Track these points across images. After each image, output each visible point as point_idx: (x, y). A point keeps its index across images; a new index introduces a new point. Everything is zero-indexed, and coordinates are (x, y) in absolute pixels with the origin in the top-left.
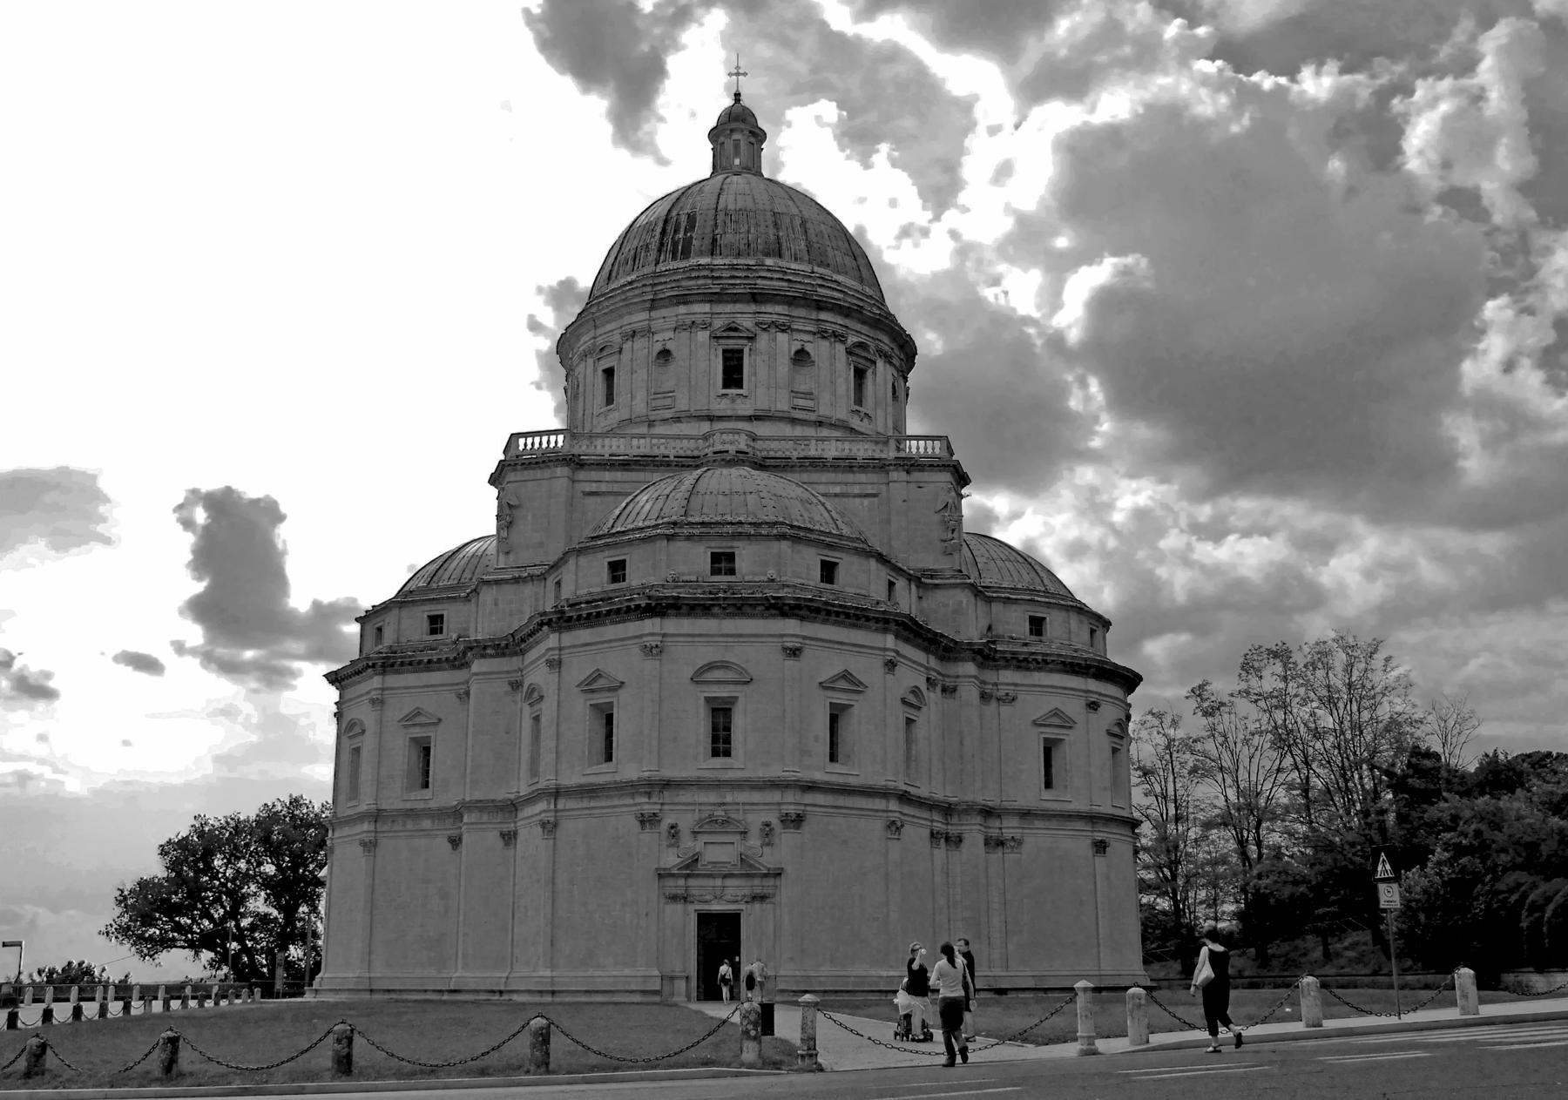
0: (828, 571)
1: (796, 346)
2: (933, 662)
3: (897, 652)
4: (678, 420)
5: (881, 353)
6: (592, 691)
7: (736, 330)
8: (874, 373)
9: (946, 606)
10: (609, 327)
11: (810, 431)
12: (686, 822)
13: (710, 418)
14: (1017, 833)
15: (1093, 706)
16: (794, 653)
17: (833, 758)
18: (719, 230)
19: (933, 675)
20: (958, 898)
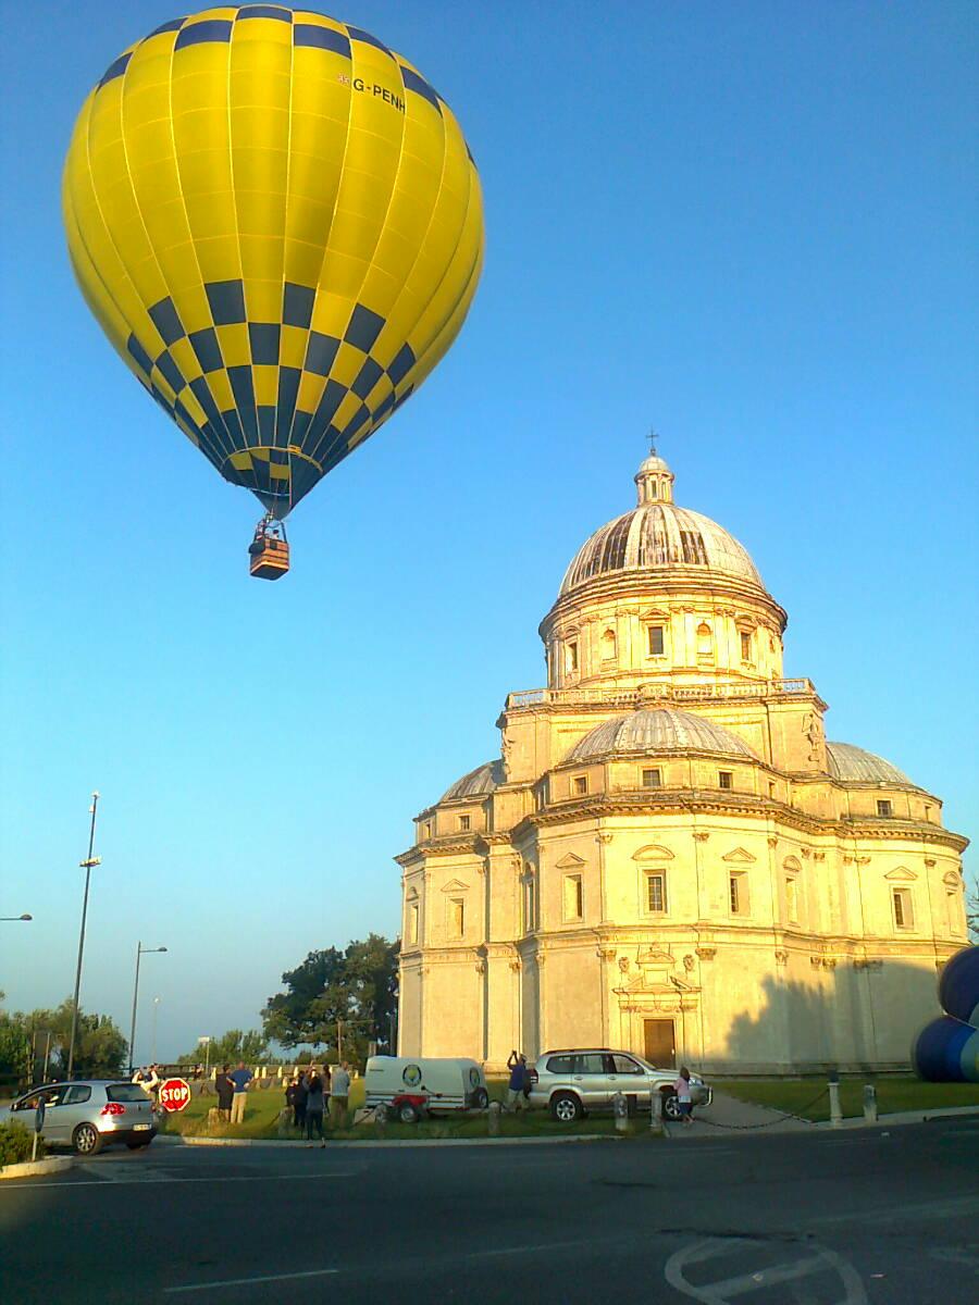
0: (725, 778)
3: (777, 833)
4: (620, 677)
5: (760, 621)
6: (567, 867)
7: (657, 614)
8: (756, 635)
10: (571, 616)
11: (712, 680)
12: (632, 956)
13: (641, 675)
15: (930, 863)
16: (703, 837)
17: (734, 909)
18: (642, 548)
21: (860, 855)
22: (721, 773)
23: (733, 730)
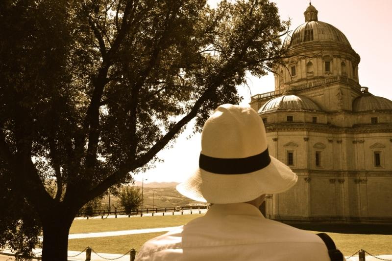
1: (308, 62)
2: (331, 135)
8: (332, 62)
9: (339, 120)
14: (365, 178)
16: (275, 140)
19: (330, 139)
20: (343, 196)
21: (360, 139)
22: (288, 117)
23: (314, 99)
